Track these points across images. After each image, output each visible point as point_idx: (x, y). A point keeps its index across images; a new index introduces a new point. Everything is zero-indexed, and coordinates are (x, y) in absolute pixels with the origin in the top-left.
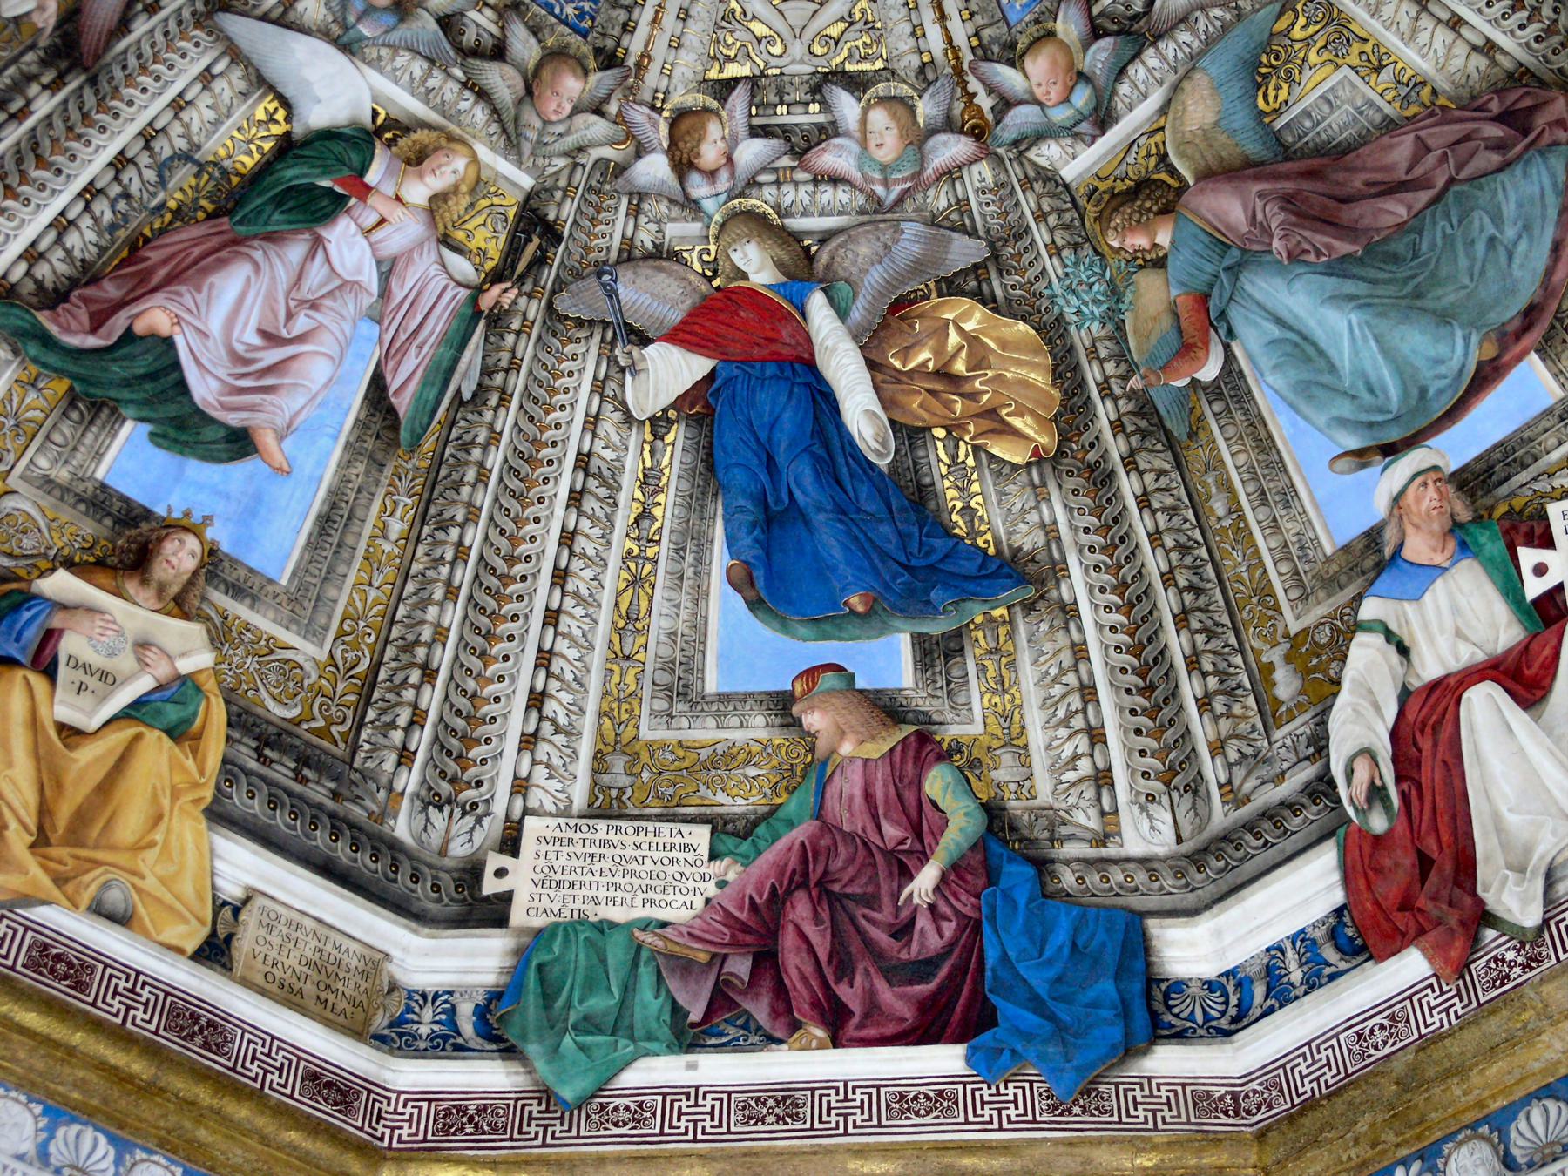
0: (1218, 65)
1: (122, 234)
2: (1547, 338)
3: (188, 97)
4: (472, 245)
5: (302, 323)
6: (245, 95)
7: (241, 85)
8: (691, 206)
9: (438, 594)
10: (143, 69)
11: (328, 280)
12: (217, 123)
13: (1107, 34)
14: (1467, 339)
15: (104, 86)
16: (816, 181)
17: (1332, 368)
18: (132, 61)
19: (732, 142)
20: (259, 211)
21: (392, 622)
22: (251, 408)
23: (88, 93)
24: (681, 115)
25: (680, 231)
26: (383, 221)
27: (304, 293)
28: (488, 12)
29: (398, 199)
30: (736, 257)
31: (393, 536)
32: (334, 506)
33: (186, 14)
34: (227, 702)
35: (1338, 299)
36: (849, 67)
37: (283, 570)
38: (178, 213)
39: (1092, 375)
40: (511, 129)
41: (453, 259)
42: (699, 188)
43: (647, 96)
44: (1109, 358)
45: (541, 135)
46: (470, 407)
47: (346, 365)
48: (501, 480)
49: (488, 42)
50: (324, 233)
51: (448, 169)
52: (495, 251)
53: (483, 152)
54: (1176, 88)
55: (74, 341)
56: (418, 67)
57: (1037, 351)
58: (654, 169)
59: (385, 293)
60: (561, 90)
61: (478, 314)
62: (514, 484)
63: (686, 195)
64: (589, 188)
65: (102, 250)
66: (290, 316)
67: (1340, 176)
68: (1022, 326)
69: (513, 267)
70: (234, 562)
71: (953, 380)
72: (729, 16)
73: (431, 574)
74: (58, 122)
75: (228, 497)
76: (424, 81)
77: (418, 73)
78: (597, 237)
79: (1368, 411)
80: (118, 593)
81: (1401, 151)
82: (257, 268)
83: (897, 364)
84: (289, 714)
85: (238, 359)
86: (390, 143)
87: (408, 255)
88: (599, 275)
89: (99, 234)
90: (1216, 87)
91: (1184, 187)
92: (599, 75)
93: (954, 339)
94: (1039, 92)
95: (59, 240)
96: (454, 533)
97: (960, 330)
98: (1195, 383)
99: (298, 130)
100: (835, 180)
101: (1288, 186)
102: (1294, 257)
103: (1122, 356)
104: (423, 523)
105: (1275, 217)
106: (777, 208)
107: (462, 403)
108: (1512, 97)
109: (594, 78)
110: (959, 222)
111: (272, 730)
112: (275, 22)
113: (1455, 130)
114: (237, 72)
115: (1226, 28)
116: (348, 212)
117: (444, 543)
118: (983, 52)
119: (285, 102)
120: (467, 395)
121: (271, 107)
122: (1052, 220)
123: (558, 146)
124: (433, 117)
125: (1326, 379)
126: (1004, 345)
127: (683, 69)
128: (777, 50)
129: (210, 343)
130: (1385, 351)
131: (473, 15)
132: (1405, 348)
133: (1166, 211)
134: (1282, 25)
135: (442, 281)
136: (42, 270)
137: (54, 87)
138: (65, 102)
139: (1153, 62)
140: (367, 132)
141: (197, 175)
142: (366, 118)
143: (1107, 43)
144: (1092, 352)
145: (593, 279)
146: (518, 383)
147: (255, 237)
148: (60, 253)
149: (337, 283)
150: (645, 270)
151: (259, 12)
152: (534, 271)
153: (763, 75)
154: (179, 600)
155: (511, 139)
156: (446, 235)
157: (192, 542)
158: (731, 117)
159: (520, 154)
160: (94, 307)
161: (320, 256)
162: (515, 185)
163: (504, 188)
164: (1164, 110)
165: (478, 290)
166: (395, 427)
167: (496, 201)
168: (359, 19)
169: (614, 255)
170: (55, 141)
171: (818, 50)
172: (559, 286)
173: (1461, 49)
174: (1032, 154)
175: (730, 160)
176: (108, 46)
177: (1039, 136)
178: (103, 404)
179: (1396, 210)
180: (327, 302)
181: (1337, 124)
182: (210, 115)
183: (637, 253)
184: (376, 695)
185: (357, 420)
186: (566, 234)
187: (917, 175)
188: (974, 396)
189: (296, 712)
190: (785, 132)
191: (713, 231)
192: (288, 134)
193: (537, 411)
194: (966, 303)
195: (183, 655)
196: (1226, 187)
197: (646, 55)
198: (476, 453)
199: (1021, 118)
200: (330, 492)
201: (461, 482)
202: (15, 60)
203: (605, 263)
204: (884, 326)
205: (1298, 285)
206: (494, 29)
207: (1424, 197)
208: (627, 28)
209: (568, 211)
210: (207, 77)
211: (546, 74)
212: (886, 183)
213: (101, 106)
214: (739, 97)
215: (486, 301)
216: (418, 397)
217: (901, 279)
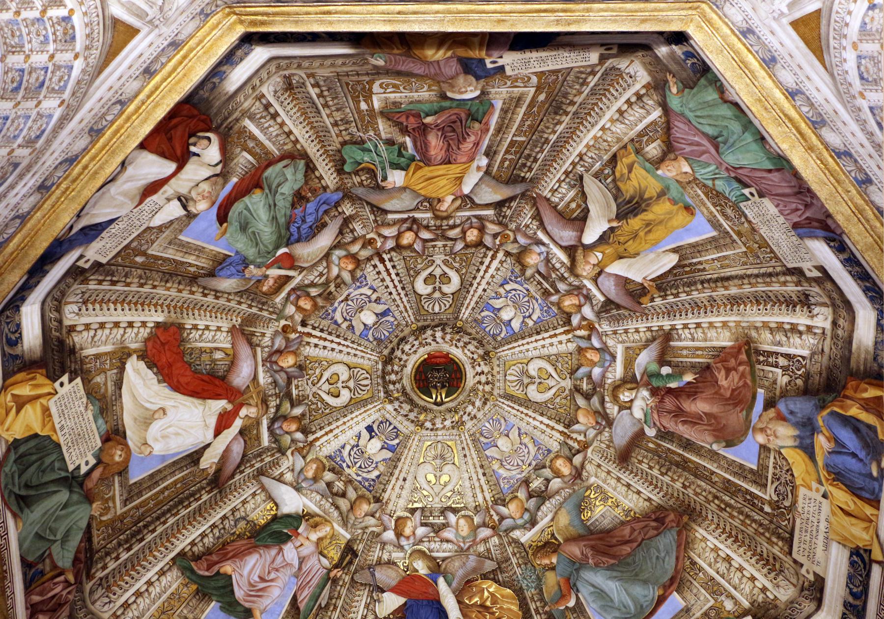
0: (569, 506)
1: (221, 540)
2: (678, 587)
4: (329, 556)
5: (272, 576)
6: (265, 501)
7: (264, 498)
8: (401, 547)
10: (236, 490)
11: (282, 562)
12: (255, 509)
13: (534, 497)
14: (653, 588)
15: (224, 494)
16: (441, 541)
17: (612, 601)
18: (233, 487)
19: (415, 528)
20: (264, 538)
23: (218, 496)
24: (399, 519)
25: (397, 555)
27: (274, 566)
30: (415, 565)
35: (611, 578)
36: (453, 506)
38: (239, 536)
39: (532, 606)
41: (323, 560)
42: (403, 542)
44: (538, 600)
49: (341, 492)
50: (283, 547)
52: (336, 558)
53: (336, 526)
54: (556, 513)
55: (201, 573)
56: (318, 497)
57: (514, 599)
58: (390, 535)
59: (300, 568)
61: (329, 578)
64: (368, 540)
65: (214, 545)
66: (269, 573)
67: (608, 539)
68: (508, 590)
71: (487, 608)
72: (416, 489)
74: (208, 503)
79: (625, 614)
81: (627, 531)
83: (467, 602)
85: (251, 585)
87: (309, 556)
88: (369, 569)
90: (569, 513)
91: (560, 544)
93: (486, 594)
94: (513, 515)
97: (488, 591)
98: (567, 607)
99: (279, 513)
100: (448, 541)
101: (593, 543)
102: (597, 565)
103: (542, 599)
105: (589, 553)
106: (429, 549)
108: (658, 514)
109: (372, 505)
110: (487, 556)
112: (279, 480)
113: (643, 524)
114: (263, 494)
115: (570, 495)
118: (496, 502)
119: (276, 505)
120: (323, 605)
122: (518, 555)
123: (359, 526)
124: (321, 513)
125: (610, 604)
126: (503, 596)
128: (430, 499)
130: (628, 594)
131: (337, 483)
132: (635, 593)
133: (554, 552)
134: (587, 494)
135: (318, 566)
136: (195, 549)
137: (209, 492)
139: (549, 505)
143: (534, 499)
144: (532, 599)
146: (340, 603)
148: (201, 544)
150: (384, 568)
155: (345, 523)
162: (345, 537)
164: (552, 520)
165: (330, 571)
166: (299, 614)
170: (206, 509)
171: (443, 500)
172: (356, 572)
173: (641, 500)
174: (511, 534)
175: (414, 533)
176: (227, 482)
177: (513, 528)
179: (627, 549)
181: (606, 523)
182: (253, 506)
187: (474, 540)
188: (493, 613)
190: (432, 525)
191: (407, 556)
192: (276, 514)
193: (345, 613)
194: (490, 582)
196: (573, 543)
197: (389, 499)
199: (507, 523)
202: (200, 482)
204: (463, 589)
205: (598, 574)
207: (635, 544)
208: (384, 491)
209: (361, 547)
210: (254, 495)
211: (357, 503)
212: (464, 543)
214: (418, 513)
215: (332, 575)
216: (307, 604)
217: (467, 574)
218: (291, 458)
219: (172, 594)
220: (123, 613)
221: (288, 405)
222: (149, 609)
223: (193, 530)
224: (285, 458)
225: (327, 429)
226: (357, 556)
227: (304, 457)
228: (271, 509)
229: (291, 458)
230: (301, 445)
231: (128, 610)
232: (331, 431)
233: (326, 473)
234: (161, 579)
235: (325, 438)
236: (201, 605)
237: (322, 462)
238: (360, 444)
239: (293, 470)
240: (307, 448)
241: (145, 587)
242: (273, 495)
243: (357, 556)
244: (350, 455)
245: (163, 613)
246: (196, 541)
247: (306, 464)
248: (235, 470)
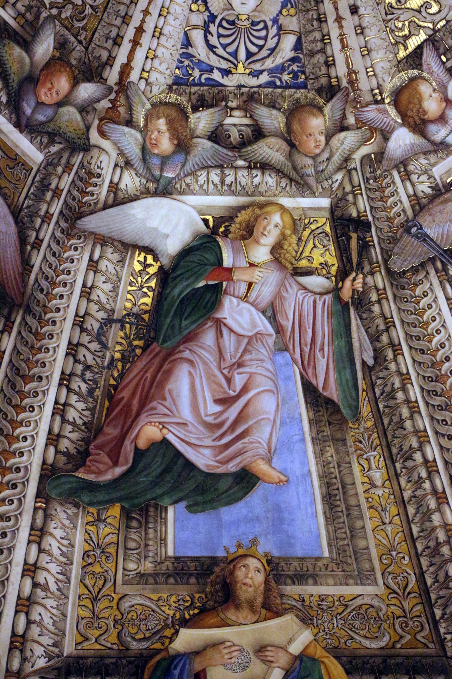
1: (98, 393)
3: (89, 284)
4: (315, 264)
6: (122, 261)
7: (116, 257)
9: (433, 504)
11: (239, 343)
12: (115, 289)
18: (44, 284)
21: (414, 541)
22: (240, 453)
23: (30, 320)
26: (250, 284)
27: (229, 361)
28: (236, 113)
29: (251, 265)
31: (379, 483)
32: (329, 485)
33: (58, 234)
34: (337, 658)
37: (321, 546)
38: (124, 359)
40: (294, 175)
43: (368, 98)
45: (316, 167)
46: (378, 368)
47: (282, 389)
48: (427, 403)
49: (248, 131)
50: (219, 315)
51: (271, 227)
53: (287, 202)
55: (108, 477)
56: (215, 176)
60: (309, 131)
61: (345, 306)
62: (437, 401)
63: (433, 143)
64: (367, 181)
65: (92, 410)
66: (229, 380)
69: (350, 260)
70: (287, 559)
73: (418, 493)
74: (21, 347)
75: (258, 519)
76: (223, 181)
77: (216, 179)
78: (391, 208)
80: (225, 624)
82: (191, 363)
84: (382, 644)
86: (226, 234)
88: (408, 231)
89: (85, 402)
92: (329, 105)
95: (64, 420)
96: (418, 456)
99: (165, 261)
104: (393, 463)
107: (370, 369)
109: (327, 110)
111: (378, 661)
114: (110, 250)
116: (226, 293)
117: (415, 467)
119: (148, 250)
120: (370, 362)
121: (141, 259)
123: (331, 168)
124: (242, 200)
127: (381, 64)
128: (435, 8)
129: (191, 428)
131: (229, 121)
135: (310, 299)
136: (64, 444)
138: (19, 333)
140: (208, 236)
141: (122, 328)
142: (202, 227)
145: (406, 236)
147: (178, 345)
148: (69, 428)
149: (246, 341)
150: (436, 208)
151: (100, 205)
152: (365, 256)
153: (435, 31)
154: (267, 606)
156: (295, 269)
157: (253, 563)
158: (431, 73)
159: (310, 188)
160: (108, 449)
161: (225, 331)
163: (313, 215)
166: (337, 410)
167: (313, 227)
168: (162, 170)
169: (410, 213)
170: (27, 361)
176: (25, 284)
178: (148, 506)
180: (247, 357)
182: (108, 287)
183: (424, 201)
184: (433, 597)
185: (310, 421)
186: (370, 219)
189: (386, 639)
192: (161, 268)
193: (423, 344)
195: (291, 641)
197: (351, 72)
198: (400, 395)
200: (320, 477)
201: (402, 421)
203: (407, 221)
206: (246, 121)
211: (296, 127)
213: (42, 322)
215: (346, 294)
216: (339, 382)
218: (105, 144)
219: (86, 554)
220: (24, 660)
221: (17, 51)
222: (64, 615)
223: (34, 416)
224: (95, 152)
225: (130, 33)
226: (367, 225)
227: (129, 123)
228: (146, 266)
229: (105, 144)
230: (105, 104)
231: (29, 645)
232: (140, 30)
233: (193, 118)
234: (45, 545)
235: (140, 54)
236: (151, 531)
237: (170, 104)
238: (214, 9)
239: (128, 164)
240: (122, 100)
241: (28, 582)
242: (129, 238)
243: (367, 225)
244: (211, 48)
245: (95, 600)
246: (56, 430)
247: (144, 131)
248: (22, 250)
